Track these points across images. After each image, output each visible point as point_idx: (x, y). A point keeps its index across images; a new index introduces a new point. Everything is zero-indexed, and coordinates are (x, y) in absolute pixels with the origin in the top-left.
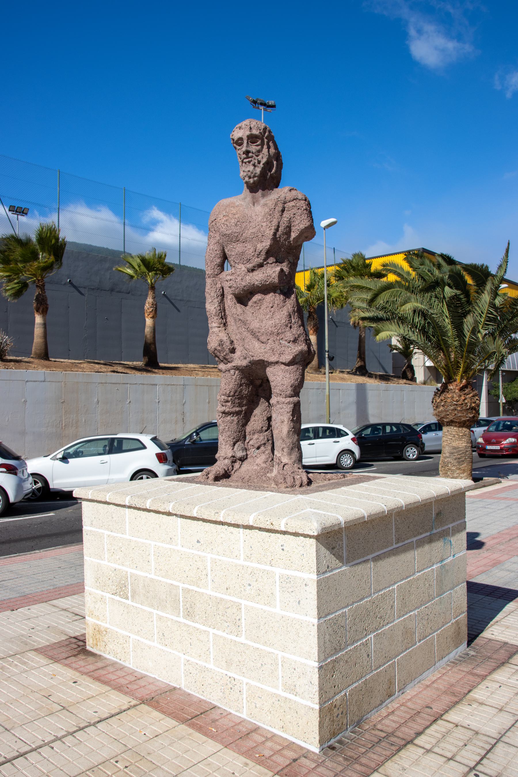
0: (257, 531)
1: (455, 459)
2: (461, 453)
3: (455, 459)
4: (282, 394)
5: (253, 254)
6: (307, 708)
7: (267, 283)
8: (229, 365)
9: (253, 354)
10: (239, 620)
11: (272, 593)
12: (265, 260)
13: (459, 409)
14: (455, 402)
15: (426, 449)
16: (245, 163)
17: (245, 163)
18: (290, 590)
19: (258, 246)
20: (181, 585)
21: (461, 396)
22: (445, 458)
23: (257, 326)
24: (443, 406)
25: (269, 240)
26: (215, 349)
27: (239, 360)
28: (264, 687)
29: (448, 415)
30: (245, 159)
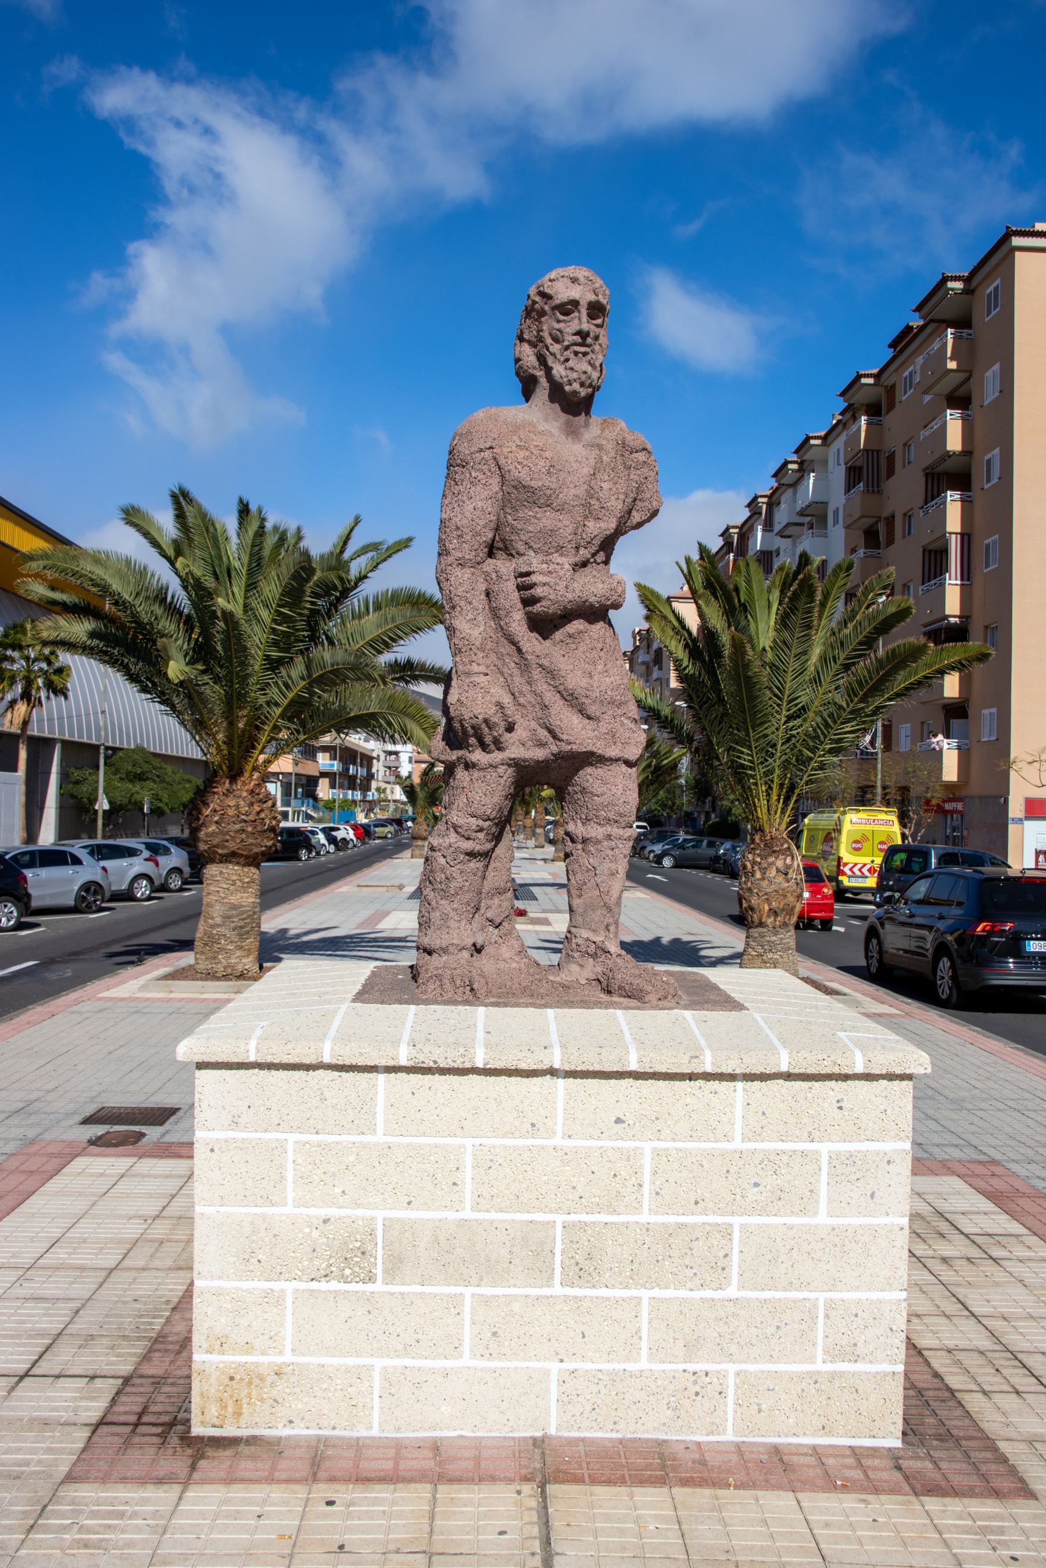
0: (781, 1081)
3: (234, 930)
4: (621, 820)
5: (570, 538)
6: (879, 1377)
7: (609, 603)
8: (497, 756)
9: (572, 739)
10: (726, 1256)
11: (811, 1191)
12: (594, 555)
13: (250, 829)
15: (35, 904)
16: (576, 353)
17: (576, 353)
18: (853, 1177)
19: (591, 524)
20: (560, 1219)
21: (252, 804)
22: (213, 927)
23: (583, 684)
24: (216, 822)
25: (614, 520)
26: (486, 721)
27: (522, 746)
28: (780, 1367)
29: (227, 841)
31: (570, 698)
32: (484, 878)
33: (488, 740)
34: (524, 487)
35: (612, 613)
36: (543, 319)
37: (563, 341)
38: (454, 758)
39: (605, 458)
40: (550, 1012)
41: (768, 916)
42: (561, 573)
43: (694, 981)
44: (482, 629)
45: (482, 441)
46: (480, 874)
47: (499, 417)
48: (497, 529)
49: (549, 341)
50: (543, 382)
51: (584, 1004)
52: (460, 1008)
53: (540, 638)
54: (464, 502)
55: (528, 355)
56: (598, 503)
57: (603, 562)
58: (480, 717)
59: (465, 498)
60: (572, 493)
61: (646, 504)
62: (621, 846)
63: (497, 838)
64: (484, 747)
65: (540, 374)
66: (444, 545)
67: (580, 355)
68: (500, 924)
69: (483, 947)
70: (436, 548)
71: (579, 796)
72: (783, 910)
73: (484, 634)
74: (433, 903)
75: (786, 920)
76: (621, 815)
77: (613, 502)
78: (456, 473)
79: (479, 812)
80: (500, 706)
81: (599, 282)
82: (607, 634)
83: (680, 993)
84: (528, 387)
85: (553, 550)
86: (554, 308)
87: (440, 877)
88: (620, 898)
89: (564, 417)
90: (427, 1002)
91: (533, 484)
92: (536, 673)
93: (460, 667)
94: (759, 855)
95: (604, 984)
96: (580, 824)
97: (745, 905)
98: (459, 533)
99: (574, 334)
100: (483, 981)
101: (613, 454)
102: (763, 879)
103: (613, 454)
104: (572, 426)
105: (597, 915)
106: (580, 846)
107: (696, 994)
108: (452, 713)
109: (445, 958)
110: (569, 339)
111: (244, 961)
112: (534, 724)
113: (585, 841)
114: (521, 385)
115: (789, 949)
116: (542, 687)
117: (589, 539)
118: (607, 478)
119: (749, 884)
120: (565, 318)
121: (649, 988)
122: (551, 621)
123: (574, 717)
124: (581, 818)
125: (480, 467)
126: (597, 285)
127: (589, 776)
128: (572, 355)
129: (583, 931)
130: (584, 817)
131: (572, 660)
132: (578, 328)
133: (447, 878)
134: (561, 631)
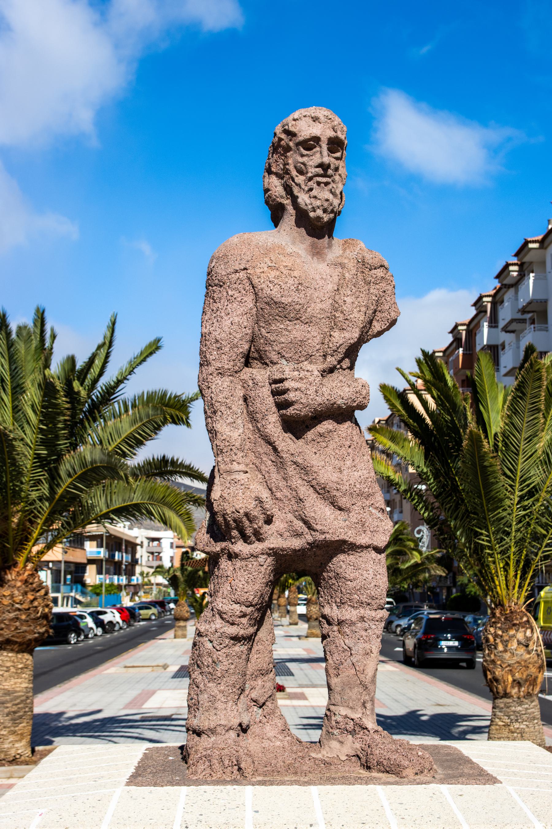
1: (8, 715)
2: (18, 701)
3: (8, 715)
4: (373, 603)
5: (318, 347)
7: (355, 404)
8: (258, 547)
9: (326, 529)
12: (340, 362)
14: (17, 606)
16: (319, 183)
17: (319, 183)
19: (336, 334)
21: (26, 593)
23: (334, 479)
25: (357, 330)
26: (247, 515)
27: (281, 536)
30: (318, 175)
31: (323, 492)
32: (248, 660)
33: (249, 531)
34: (276, 303)
35: (357, 413)
36: (288, 154)
37: (307, 173)
38: (218, 549)
39: (347, 275)
40: (314, 789)
41: (513, 687)
42: (311, 379)
43: (448, 754)
44: (241, 431)
45: (237, 263)
46: (244, 657)
47: (252, 241)
48: (252, 341)
49: (294, 173)
50: (290, 209)
51: (346, 780)
52: (229, 787)
53: (293, 438)
54: (222, 318)
55: (276, 186)
56: (342, 315)
57: (348, 368)
58: (242, 511)
59: (223, 314)
60: (318, 306)
61: (385, 314)
62: (374, 627)
63: (259, 623)
64: (245, 539)
65: (287, 202)
66: (205, 357)
67: (323, 185)
68: (264, 704)
69: (248, 726)
70: (198, 360)
71: (334, 581)
72: (526, 680)
73: (243, 436)
74: (201, 686)
75: (530, 690)
76: (372, 598)
77: (356, 314)
78: (214, 292)
79: (242, 599)
80: (259, 500)
81: (337, 120)
82: (354, 433)
83: (435, 767)
84: (276, 214)
85: (303, 359)
86: (298, 144)
87: (207, 660)
88: (374, 676)
89: (309, 240)
90: (197, 783)
91: (283, 300)
92: (291, 470)
93: (222, 467)
94: (500, 628)
95: (364, 759)
96: (335, 607)
97: (489, 676)
98: (218, 345)
99: (317, 167)
100: (249, 760)
101: (354, 272)
102: (505, 651)
103: (354, 272)
104: (316, 248)
105: (355, 693)
106: (335, 628)
107: (450, 767)
108: (216, 508)
109: (213, 738)
110: (312, 171)
111: (17, 745)
112: (290, 516)
113: (340, 623)
114: (270, 212)
115: (534, 718)
116: (297, 482)
117: (335, 348)
118: (349, 293)
119: (492, 656)
120: (308, 152)
121: (406, 763)
122: (303, 422)
123: (327, 509)
124: (336, 602)
125: (236, 286)
126: (336, 123)
127: (342, 563)
128: (315, 185)
129: (341, 708)
130: (338, 600)
131: (323, 457)
132: (319, 161)
133: (214, 662)
134: (312, 431)
